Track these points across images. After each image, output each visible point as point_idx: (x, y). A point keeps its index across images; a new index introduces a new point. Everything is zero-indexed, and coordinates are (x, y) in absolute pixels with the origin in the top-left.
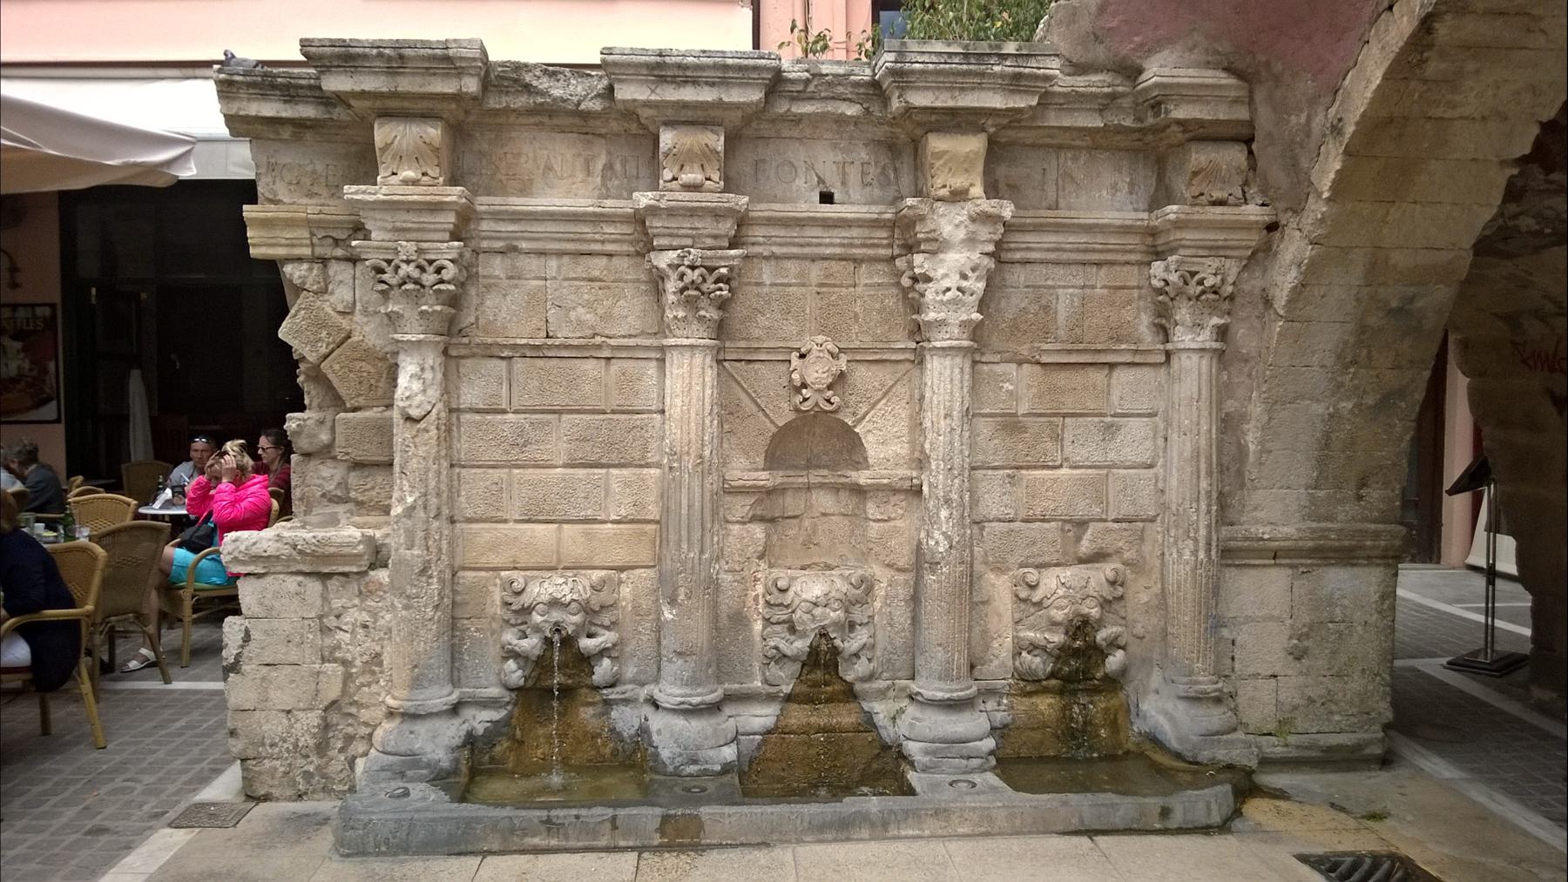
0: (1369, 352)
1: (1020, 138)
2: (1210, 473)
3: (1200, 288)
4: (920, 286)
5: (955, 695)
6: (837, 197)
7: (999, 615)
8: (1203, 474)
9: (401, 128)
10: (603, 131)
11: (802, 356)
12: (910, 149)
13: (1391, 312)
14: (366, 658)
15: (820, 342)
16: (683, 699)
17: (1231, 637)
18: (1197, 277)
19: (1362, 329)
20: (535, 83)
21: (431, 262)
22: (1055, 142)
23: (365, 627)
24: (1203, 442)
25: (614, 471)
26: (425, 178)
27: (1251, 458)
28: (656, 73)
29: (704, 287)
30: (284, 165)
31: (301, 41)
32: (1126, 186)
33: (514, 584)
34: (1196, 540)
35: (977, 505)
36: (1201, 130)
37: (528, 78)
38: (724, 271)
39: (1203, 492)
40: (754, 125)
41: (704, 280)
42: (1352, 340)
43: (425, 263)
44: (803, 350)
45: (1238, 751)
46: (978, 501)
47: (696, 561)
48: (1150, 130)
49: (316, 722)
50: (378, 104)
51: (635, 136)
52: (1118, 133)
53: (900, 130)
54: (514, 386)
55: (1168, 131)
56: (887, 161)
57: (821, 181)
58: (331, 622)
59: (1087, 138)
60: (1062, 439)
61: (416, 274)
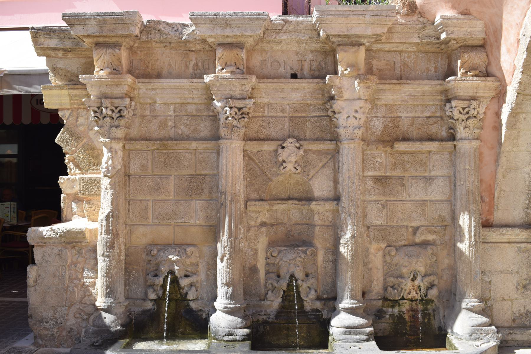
1: (383, 48)
3: (467, 116)
4: (337, 116)
5: (354, 305)
6: (299, 75)
7: (377, 269)
9: (104, 50)
10: (193, 49)
11: (283, 148)
12: (332, 54)
15: (291, 142)
16: (227, 305)
17: (489, 280)
18: (466, 110)
20: (162, 29)
21: (116, 108)
22: (399, 49)
25: (197, 202)
26: (115, 71)
28: (215, 23)
29: (236, 117)
31: (63, 14)
32: (433, 69)
33: (152, 252)
35: (366, 218)
36: (465, 42)
37: (160, 27)
38: (245, 110)
40: (260, 44)
41: (236, 114)
44: (284, 145)
45: (491, 335)
46: (366, 216)
47: (233, 242)
48: (443, 43)
50: (95, 40)
51: (208, 51)
52: (428, 45)
53: (327, 45)
55: (450, 43)
56: (321, 59)
59: (414, 47)
60: (406, 186)
61: (110, 113)
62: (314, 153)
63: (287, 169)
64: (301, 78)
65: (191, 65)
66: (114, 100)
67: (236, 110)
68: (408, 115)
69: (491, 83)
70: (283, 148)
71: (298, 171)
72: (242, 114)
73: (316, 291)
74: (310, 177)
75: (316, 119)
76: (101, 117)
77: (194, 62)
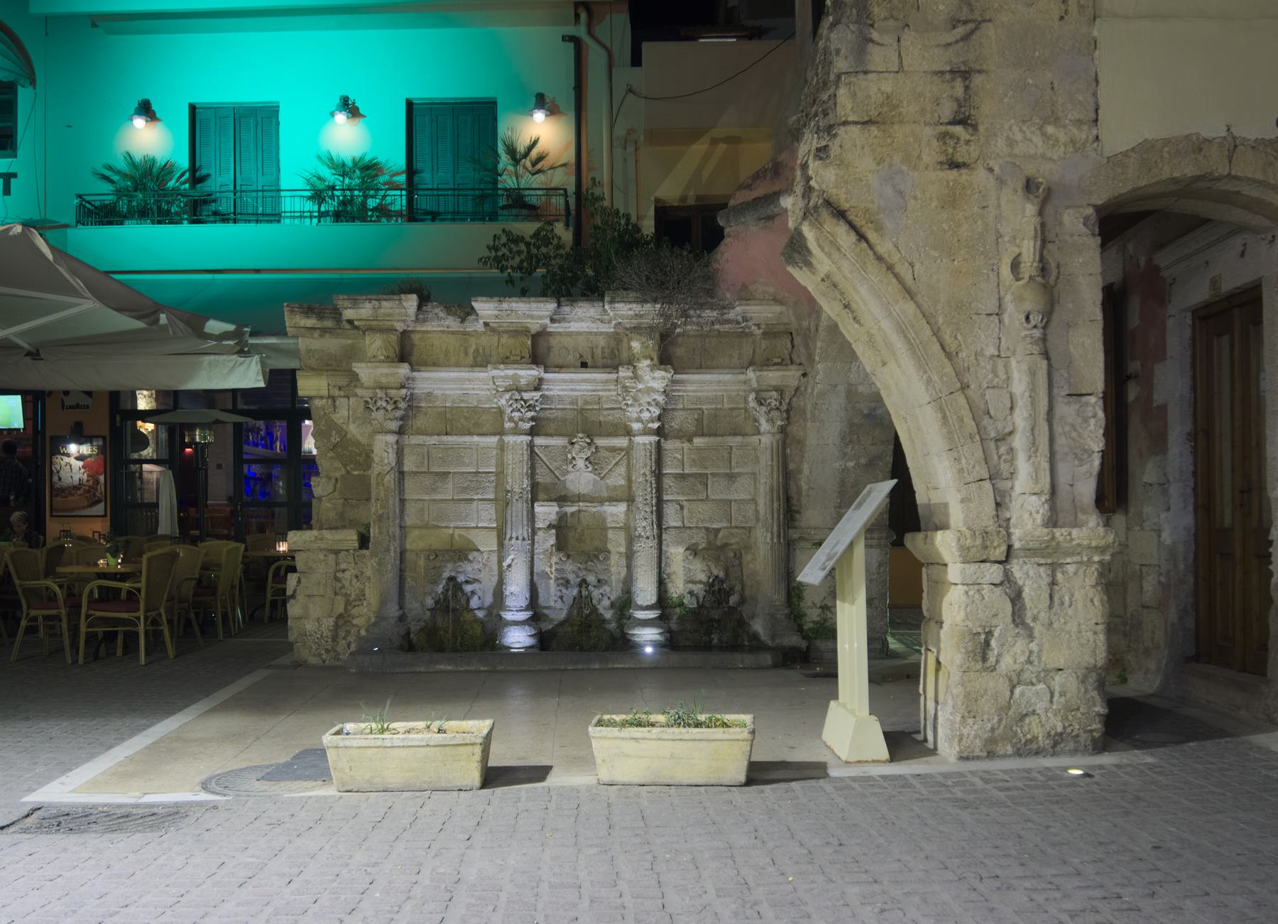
0: (858, 437)
2: (779, 500)
8: (775, 499)
11: (573, 444)
13: (868, 416)
14: (357, 592)
19: (851, 425)
23: (357, 577)
24: (775, 483)
27: (804, 493)
30: (315, 350)
34: (772, 533)
39: (775, 509)
41: (522, 406)
42: (847, 430)
43: (388, 399)
49: (332, 624)
54: (430, 458)
57: (581, 356)
58: (339, 575)
61: (384, 404)
62: (606, 450)
63: (577, 467)
64: (592, 367)
65: (472, 350)
66: (389, 391)
67: (523, 403)
68: (709, 407)
69: (794, 372)
70: (573, 444)
71: (589, 470)
72: (528, 407)
73: (609, 598)
74: (602, 475)
75: (608, 412)
76: (374, 409)
77: (474, 347)
